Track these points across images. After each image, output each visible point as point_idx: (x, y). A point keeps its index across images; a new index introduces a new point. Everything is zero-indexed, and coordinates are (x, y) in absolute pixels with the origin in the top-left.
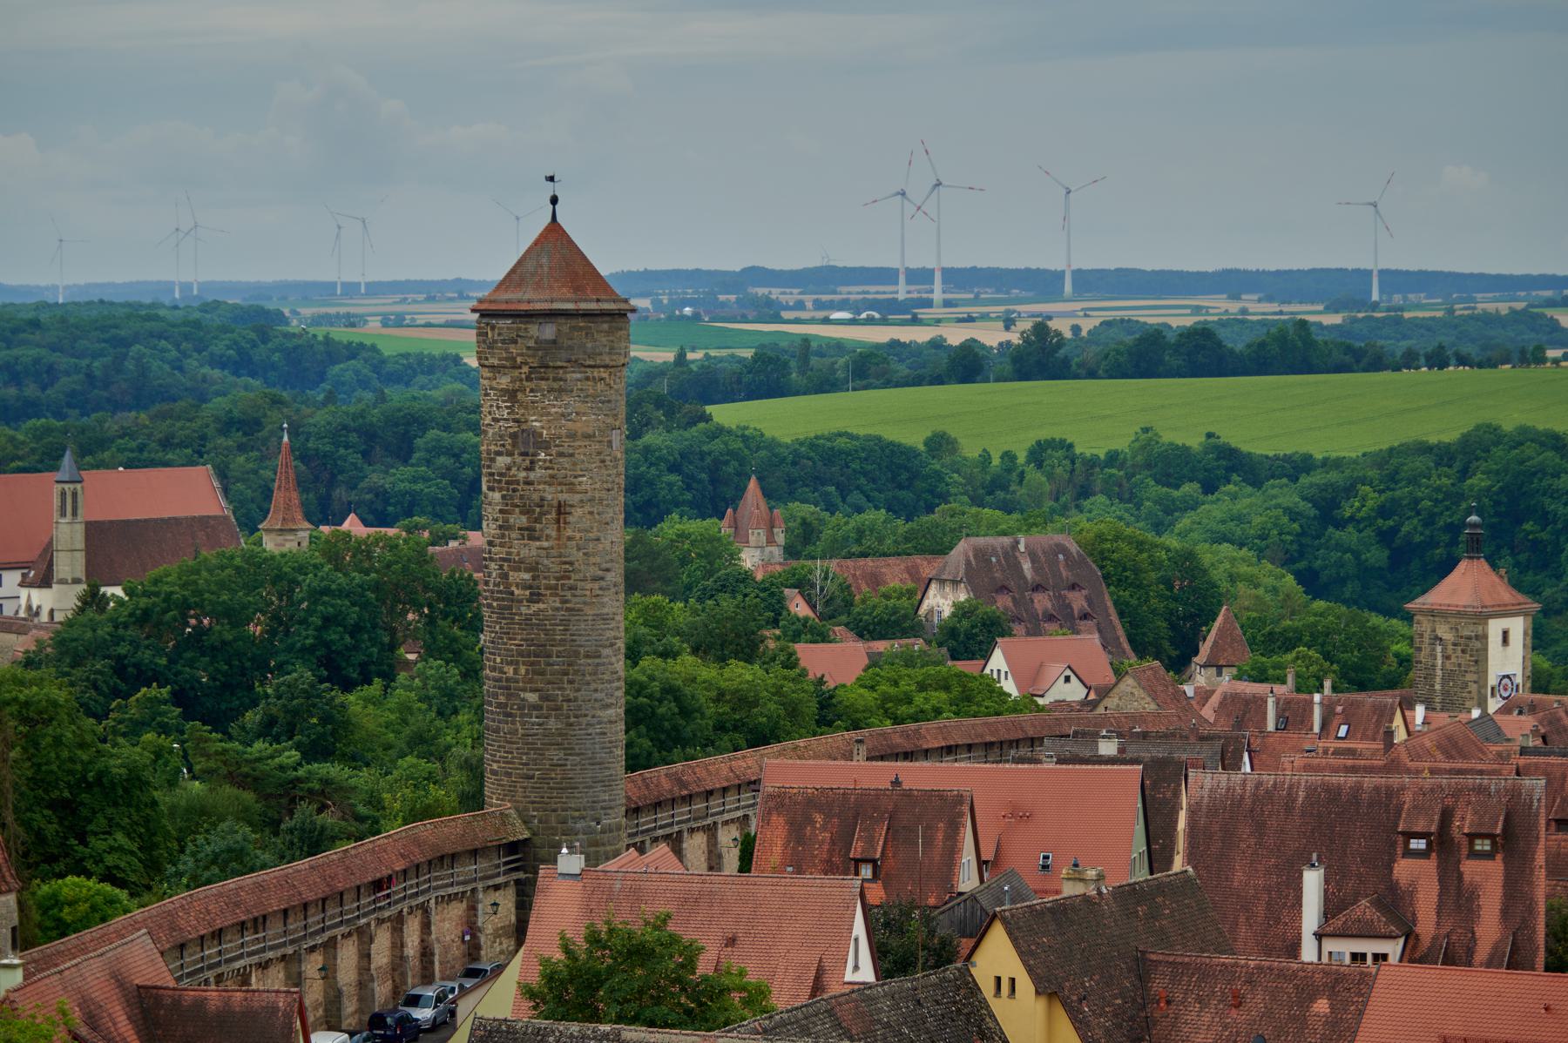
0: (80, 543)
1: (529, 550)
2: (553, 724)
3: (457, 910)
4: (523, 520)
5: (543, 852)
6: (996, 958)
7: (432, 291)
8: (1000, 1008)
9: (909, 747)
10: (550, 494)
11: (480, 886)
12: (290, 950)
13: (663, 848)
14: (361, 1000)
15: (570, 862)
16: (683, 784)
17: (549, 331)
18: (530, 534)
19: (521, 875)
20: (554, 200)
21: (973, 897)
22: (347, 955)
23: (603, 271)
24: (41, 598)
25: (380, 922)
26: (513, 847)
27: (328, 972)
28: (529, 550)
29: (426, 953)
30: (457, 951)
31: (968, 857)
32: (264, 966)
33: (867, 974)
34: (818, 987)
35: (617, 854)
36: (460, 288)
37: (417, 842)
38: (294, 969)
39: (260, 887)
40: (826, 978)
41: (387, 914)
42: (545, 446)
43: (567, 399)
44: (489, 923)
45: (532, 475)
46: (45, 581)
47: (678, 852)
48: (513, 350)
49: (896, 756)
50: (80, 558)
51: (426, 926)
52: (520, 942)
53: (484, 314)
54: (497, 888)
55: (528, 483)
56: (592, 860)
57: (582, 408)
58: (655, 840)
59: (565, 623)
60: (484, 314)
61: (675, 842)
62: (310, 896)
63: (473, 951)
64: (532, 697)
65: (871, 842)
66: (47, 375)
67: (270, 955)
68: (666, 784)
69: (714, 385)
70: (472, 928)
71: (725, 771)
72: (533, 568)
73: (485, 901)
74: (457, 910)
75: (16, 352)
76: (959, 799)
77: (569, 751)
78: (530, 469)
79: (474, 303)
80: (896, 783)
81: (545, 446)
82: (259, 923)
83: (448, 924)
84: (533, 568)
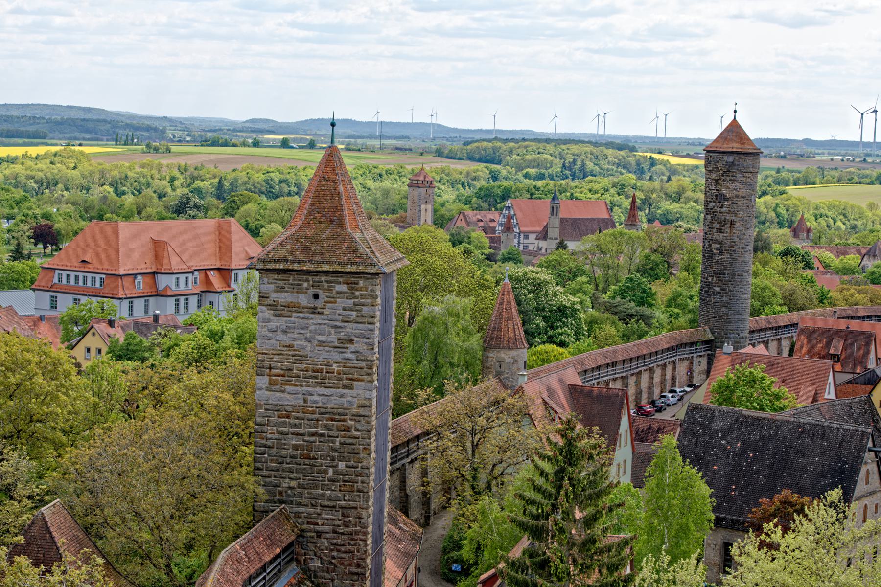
1: (720, 237)
2: (725, 299)
3: (686, 363)
4: (718, 226)
5: (718, 345)
9: (853, 314)
10: (729, 217)
11: (695, 355)
12: (624, 374)
13: (762, 346)
14: (649, 393)
15: (728, 348)
16: (769, 322)
17: (731, 159)
18: (720, 231)
19: (710, 352)
20: (735, 112)
21: (873, 371)
22: (645, 377)
23: (752, 137)
24: (543, 244)
25: (658, 366)
26: (707, 342)
27: (638, 384)
28: (720, 237)
29: (673, 379)
30: (685, 378)
31: (872, 355)
32: (615, 380)
33: (832, 396)
34: (814, 400)
35: (745, 347)
36: (699, 142)
37: (672, 338)
38: (625, 381)
39: (615, 352)
40: (818, 396)
41: (660, 363)
42: (727, 199)
43: (736, 183)
44: (697, 369)
45: (722, 210)
46: (545, 238)
47: (767, 347)
48: (718, 165)
49: (848, 318)
51: (674, 368)
52: (708, 376)
53: (708, 151)
54: (701, 356)
55: (721, 213)
57: (742, 187)
58: (759, 343)
59: (731, 263)
60: (708, 151)
61: (766, 344)
62: (633, 356)
63: (691, 378)
64: (718, 289)
65: (837, 347)
67: (617, 375)
68: (764, 323)
70: (690, 370)
71: (786, 320)
72: (721, 243)
73: (696, 361)
74: (686, 363)
76: (870, 335)
77: (730, 309)
78: (722, 208)
79: (704, 147)
80: (848, 327)
81: (727, 199)
82: (614, 364)
83: (682, 369)
84: (721, 243)
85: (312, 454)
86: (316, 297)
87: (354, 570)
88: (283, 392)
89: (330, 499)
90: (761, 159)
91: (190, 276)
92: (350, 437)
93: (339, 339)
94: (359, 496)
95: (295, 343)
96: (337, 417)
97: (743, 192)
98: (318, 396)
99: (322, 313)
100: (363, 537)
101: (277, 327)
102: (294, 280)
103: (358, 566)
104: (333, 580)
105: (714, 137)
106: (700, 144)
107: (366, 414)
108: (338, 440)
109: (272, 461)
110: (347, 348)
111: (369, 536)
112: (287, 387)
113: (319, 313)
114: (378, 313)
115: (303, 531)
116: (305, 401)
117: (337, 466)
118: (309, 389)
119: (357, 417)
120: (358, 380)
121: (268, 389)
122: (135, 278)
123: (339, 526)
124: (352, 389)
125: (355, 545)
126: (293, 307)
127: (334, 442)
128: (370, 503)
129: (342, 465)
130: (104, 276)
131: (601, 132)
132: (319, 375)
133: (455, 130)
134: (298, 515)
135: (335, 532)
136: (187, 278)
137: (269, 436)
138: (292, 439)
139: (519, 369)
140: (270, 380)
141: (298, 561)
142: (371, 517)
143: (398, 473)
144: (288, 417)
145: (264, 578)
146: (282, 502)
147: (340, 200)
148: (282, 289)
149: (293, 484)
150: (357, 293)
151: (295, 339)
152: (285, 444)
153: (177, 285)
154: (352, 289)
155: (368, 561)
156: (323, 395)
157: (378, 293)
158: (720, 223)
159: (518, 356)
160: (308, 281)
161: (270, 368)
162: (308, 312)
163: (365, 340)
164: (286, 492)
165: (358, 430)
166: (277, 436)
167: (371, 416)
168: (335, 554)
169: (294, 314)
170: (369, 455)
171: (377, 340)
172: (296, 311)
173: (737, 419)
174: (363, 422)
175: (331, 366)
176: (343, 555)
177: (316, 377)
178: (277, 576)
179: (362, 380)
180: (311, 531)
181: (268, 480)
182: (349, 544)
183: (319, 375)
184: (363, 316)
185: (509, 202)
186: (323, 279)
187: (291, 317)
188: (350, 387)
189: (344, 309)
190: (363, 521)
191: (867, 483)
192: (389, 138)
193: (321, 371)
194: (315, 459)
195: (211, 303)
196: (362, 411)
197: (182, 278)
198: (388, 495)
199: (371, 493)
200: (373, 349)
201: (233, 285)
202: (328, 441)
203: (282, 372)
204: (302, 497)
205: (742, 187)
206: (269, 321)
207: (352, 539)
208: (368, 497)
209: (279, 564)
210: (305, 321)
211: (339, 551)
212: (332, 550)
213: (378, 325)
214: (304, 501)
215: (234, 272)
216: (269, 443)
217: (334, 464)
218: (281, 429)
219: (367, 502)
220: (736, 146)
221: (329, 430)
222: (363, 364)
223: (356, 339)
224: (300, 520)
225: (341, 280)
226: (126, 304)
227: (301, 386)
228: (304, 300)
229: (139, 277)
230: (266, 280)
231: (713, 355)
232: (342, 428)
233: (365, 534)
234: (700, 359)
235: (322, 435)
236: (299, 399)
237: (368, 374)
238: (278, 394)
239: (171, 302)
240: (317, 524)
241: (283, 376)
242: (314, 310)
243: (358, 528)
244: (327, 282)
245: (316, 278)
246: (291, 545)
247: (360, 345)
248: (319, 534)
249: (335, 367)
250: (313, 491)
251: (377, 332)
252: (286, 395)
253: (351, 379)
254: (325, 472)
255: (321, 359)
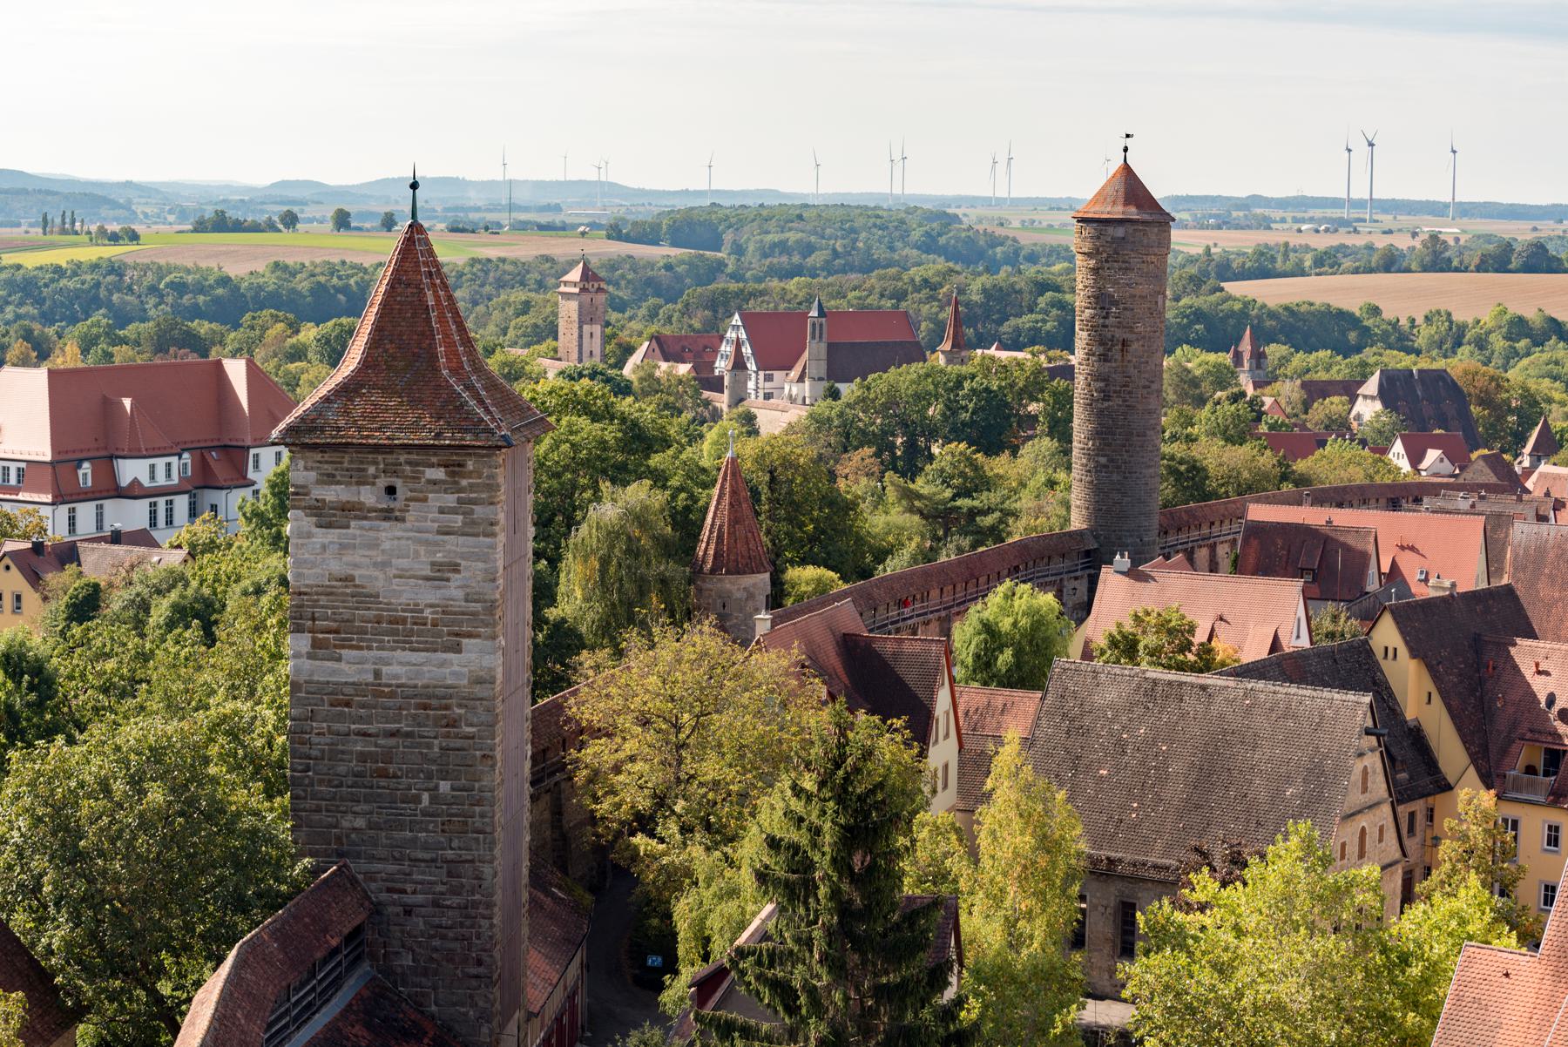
0: (823, 355)
2: (1115, 477)
6: (1386, 634)
7: (1055, 206)
8: (1387, 666)
10: (1119, 334)
11: (1065, 576)
12: (943, 614)
26: (1088, 553)
32: (927, 623)
34: (1275, 645)
36: (1069, 203)
42: (1116, 303)
50: (824, 365)
54: (1076, 578)
55: (1104, 326)
56: (1135, 562)
57: (1140, 280)
64: (1103, 460)
66: (808, 249)
69: (1226, 270)
73: (1069, 585)
75: (787, 235)
81: (1116, 303)
85: (392, 769)
86: (391, 490)
87: (473, 971)
88: (339, 659)
89: (426, 847)
90: (1173, 232)
91: (174, 460)
92: (457, 736)
93: (433, 564)
94: (477, 840)
95: (357, 573)
96: (434, 702)
97: (1144, 289)
98: (403, 666)
99: (403, 520)
100: (485, 912)
101: (324, 547)
102: (351, 462)
103: (479, 963)
104: (435, 988)
105: (1090, 196)
106: (1071, 208)
107: (485, 695)
108: (436, 742)
109: (321, 782)
110: (448, 580)
111: (496, 909)
112: (344, 652)
113: (397, 519)
114: (501, 517)
115: (380, 903)
116: (377, 674)
117: (437, 787)
118: (384, 654)
119: (468, 701)
120: (470, 635)
121: (310, 656)
122: (79, 467)
123: (442, 894)
124: (460, 652)
125: (472, 926)
126: (350, 511)
127: (430, 746)
128: (497, 852)
129: (445, 786)
130: (23, 465)
131: (897, 191)
132: (404, 628)
133: (642, 193)
134: (370, 876)
135: (436, 904)
136: (169, 465)
137: (315, 739)
138: (356, 742)
139: (757, 611)
140: (314, 640)
141: (373, 957)
142: (499, 879)
143: (547, 798)
144: (348, 704)
145: (313, 989)
146: (341, 855)
147: (428, 320)
148: (329, 479)
149: (360, 823)
150: (464, 482)
151: (356, 566)
152: (343, 752)
153: (153, 478)
154: (452, 474)
155: (497, 954)
156: (408, 664)
157: (501, 480)
158: (1102, 343)
159: (754, 585)
160: (376, 463)
161: (314, 619)
162: (377, 518)
163: (480, 565)
164: (348, 836)
165: (472, 725)
166: (327, 739)
167: (494, 698)
168: (436, 943)
169: (353, 523)
170: (493, 766)
171: (500, 564)
172: (356, 518)
173: (1139, 687)
174: (480, 710)
175: (422, 611)
176: (452, 945)
177: (394, 633)
178: (336, 984)
179: (478, 636)
180: (394, 903)
181: (316, 817)
182: (462, 925)
183: (404, 628)
184: (474, 523)
185: (737, 316)
186: (402, 458)
187: (348, 527)
188: (457, 649)
189: (442, 511)
190: (485, 884)
191: (1365, 790)
192: (526, 209)
193: (404, 621)
194: (395, 776)
195: (214, 508)
196: (478, 690)
197: (160, 463)
198: (528, 838)
199: (499, 834)
200: (494, 580)
201: (251, 475)
202: (419, 745)
203: (334, 625)
204: (376, 845)
205: (1140, 280)
206: (309, 535)
207: (468, 917)
208: (493, 843)
209: (340, 963)
210: (371, 533)
211: (444, 937)
212: (432, 937)
213: (501, 538)
214: (380, 852)
215: (252, 451)
216: (314, 753)
217: (431, 785)
218: (337, 726)
219: (491, 850)
220: (1133, 212)
221: (419, 725)
222: (478, 607)
223: (463, 563)
224: (373, 886)
225: (434, 460)
226: (63, 510)
227: (370, 648)
228: (369, 496)
229: (86, 465)
230: (301, 464)
231: (1098, 575)
232: (444, 722)
233: (490, 905)
234: (1076, 584)
235: (409, 735)
236: (366, 671)
237: (487, 626)
238: (329, 664)
239: (143, 506)
240: (404, 892)
241: (337, 632)
242: (387, 515)
243: (477, 897)
244: (409, 463)
245: (390, 458)
246: (358, 931)
247: (472, 571)
248: (408, 912)
249: (427, 613)
250: (397, 835)
251: (500, 548)
252: (343, 666)
253: (457, 635)
254: (417, 800)
255: (403, 600)
